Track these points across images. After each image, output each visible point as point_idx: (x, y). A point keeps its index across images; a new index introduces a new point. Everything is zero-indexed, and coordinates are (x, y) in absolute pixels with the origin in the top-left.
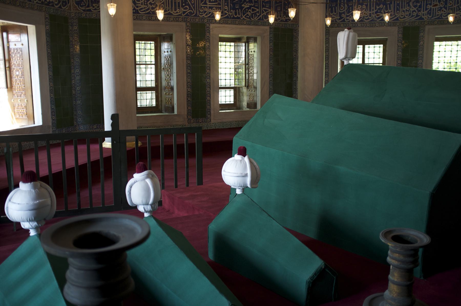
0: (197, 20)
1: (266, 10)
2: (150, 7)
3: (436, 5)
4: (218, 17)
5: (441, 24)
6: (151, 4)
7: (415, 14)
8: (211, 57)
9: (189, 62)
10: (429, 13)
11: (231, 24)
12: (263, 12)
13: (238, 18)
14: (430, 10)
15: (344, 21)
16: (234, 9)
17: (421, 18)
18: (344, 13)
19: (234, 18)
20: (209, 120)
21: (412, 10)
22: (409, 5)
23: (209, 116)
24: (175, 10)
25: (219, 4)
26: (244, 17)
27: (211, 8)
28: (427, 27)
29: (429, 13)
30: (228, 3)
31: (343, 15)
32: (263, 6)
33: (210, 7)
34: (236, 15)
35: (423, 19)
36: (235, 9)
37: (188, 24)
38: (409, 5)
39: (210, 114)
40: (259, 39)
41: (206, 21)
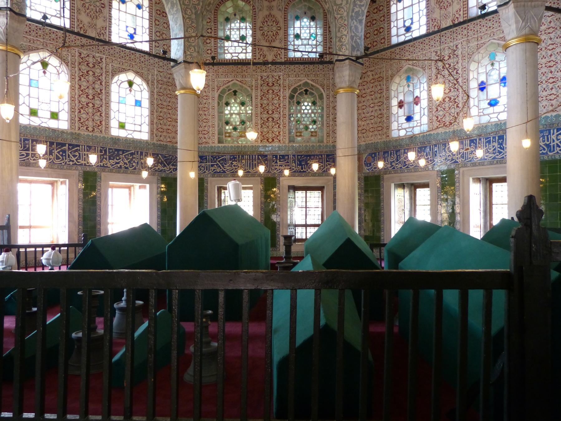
0: (270, 175)
1: (329, 164)
2: (234, 168)
3: (468, 149)
4: (287, 172)
5: (473, 166)
6: (235, 166)
7: (450, 158)
8: (281, 202)
9: (262, 205)
11: (298, 176)
12: (327, 166)
13: (304, 172)
14: (463, 154)
15: (394, 168)
16: (300, 165)
17: (456, 162)
18: (394, 161)
19: (300, 172)
20: (278, 249)
21: (447, 155)
22: (445, 151)
23: (278, 246)
24: (253, 169)
25: (288, 162)
26: (309, 171)
27: (281, 166)
30: (295, 161)
31: (393, 164)
32: (327, 161)
33: (280, 165)
34: (302, 169)
35: (457, 162)
36: (302, 165)
37: (262, 178)
38: (445, 151)
39: (279, 245)
41: (276, 175)
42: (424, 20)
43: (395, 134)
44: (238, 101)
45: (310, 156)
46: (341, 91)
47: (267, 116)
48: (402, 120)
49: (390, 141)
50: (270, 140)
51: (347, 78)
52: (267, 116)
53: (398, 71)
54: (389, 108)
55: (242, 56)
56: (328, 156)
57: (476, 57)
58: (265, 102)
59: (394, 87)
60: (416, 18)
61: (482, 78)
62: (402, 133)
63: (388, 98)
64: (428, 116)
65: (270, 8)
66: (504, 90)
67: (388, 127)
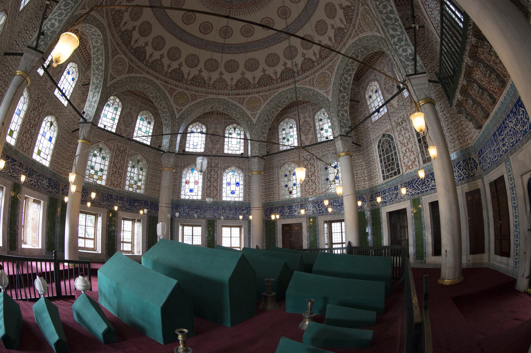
10: (218, 215)
16: (130, 205)
28: (218, 221)
29: (218, 215)
40: (142, 221)
42: (203, 146)
43: (183, 197)
44: (101, 155)
45: (136, 200)
46: (166, 169)
47: (116, 170)
48: (187, 190)
49: (180, 200)
50: (115, 186)
51: (172, 163)
52: (116, 170)
53: (188, 165)
54: (180, 182)
55: (109, 129)
56: (145, 202)
57: (227, 171)
58: (116, 161)
59: (184, 172)
60: (199, 143)
61: (229, 180)
62: (187, 197)
63: (181, 178)
64: (202, 192)
65: (131, 109)
66: (238, 188)
67: (179, 193)
